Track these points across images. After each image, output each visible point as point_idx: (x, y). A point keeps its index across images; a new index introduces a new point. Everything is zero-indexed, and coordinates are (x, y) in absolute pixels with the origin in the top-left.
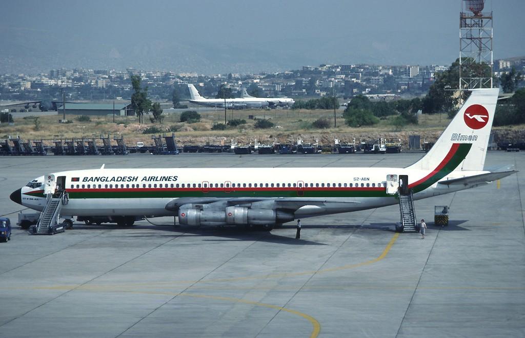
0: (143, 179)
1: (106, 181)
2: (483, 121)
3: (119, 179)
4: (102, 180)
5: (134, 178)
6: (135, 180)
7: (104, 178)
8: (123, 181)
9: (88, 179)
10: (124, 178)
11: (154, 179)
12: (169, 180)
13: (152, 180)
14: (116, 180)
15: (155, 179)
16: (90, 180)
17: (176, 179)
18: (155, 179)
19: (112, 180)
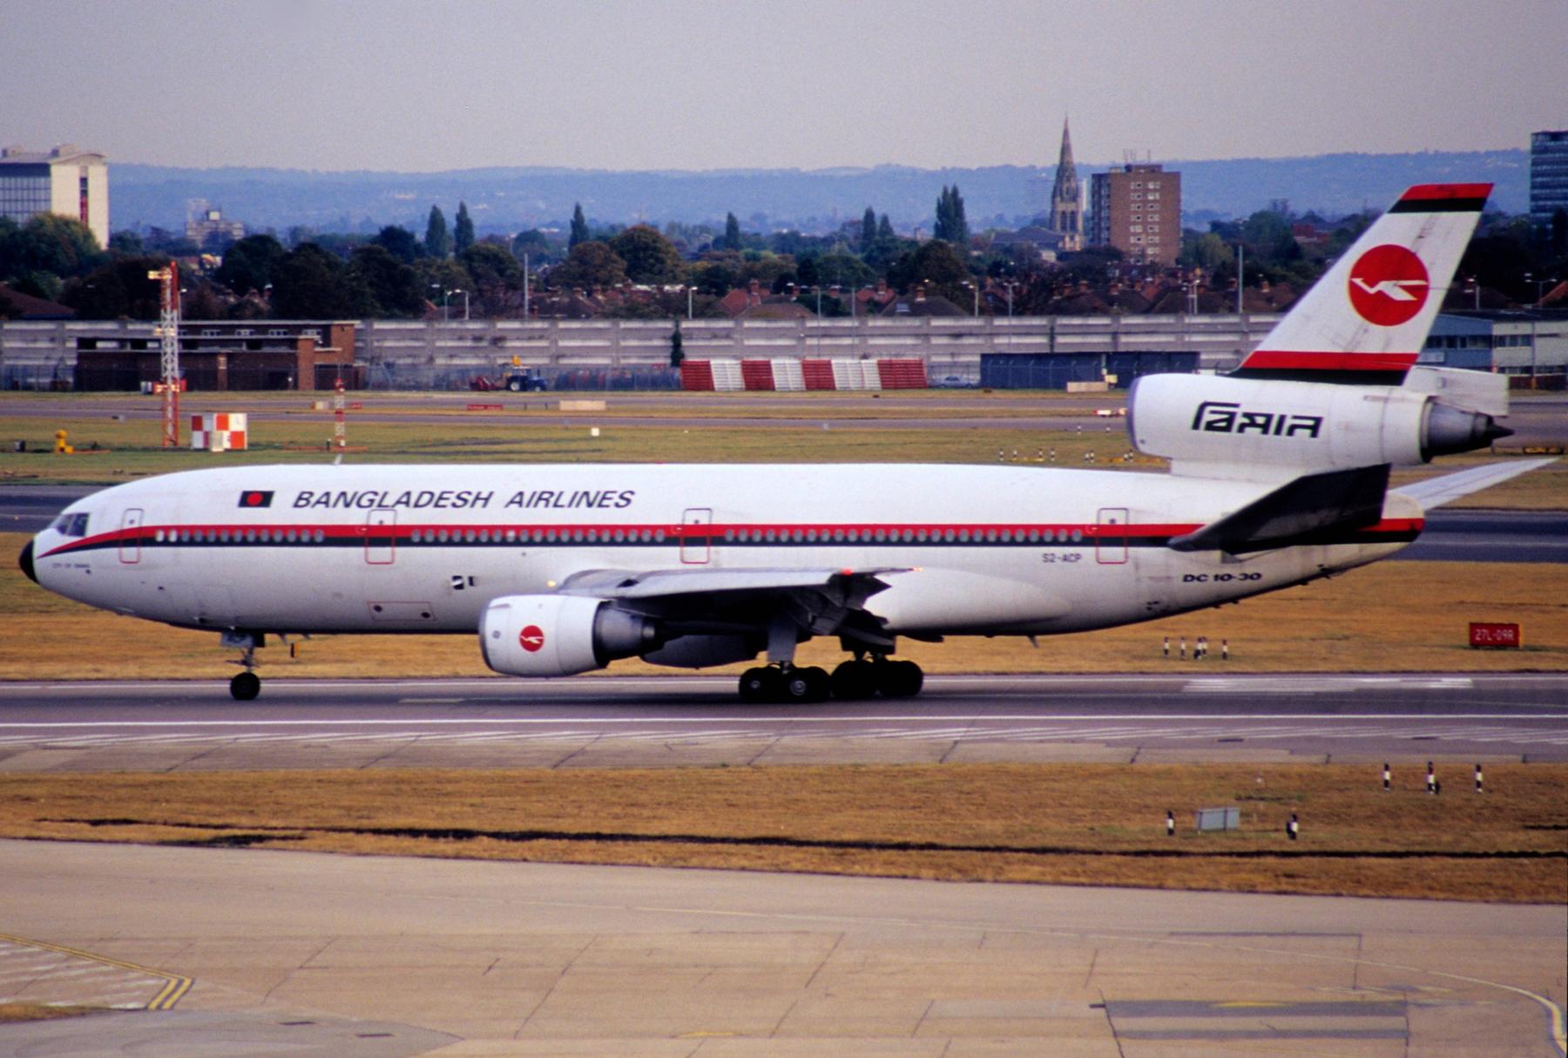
0: (512, 502)
3: (426, 498)
4: (364, 502)
5: (477, 498)
6: (480, 503)
7: (371, 496)
8: (436, 505)
9: (313, 500)
10: (441, 498)
12: (600, 505)
13: (542, 503)
14: (413, 500)
15: (552, 500)
16: (318, 502)
17: (628, 501)
18: (552, 500)
19: (399, 502)
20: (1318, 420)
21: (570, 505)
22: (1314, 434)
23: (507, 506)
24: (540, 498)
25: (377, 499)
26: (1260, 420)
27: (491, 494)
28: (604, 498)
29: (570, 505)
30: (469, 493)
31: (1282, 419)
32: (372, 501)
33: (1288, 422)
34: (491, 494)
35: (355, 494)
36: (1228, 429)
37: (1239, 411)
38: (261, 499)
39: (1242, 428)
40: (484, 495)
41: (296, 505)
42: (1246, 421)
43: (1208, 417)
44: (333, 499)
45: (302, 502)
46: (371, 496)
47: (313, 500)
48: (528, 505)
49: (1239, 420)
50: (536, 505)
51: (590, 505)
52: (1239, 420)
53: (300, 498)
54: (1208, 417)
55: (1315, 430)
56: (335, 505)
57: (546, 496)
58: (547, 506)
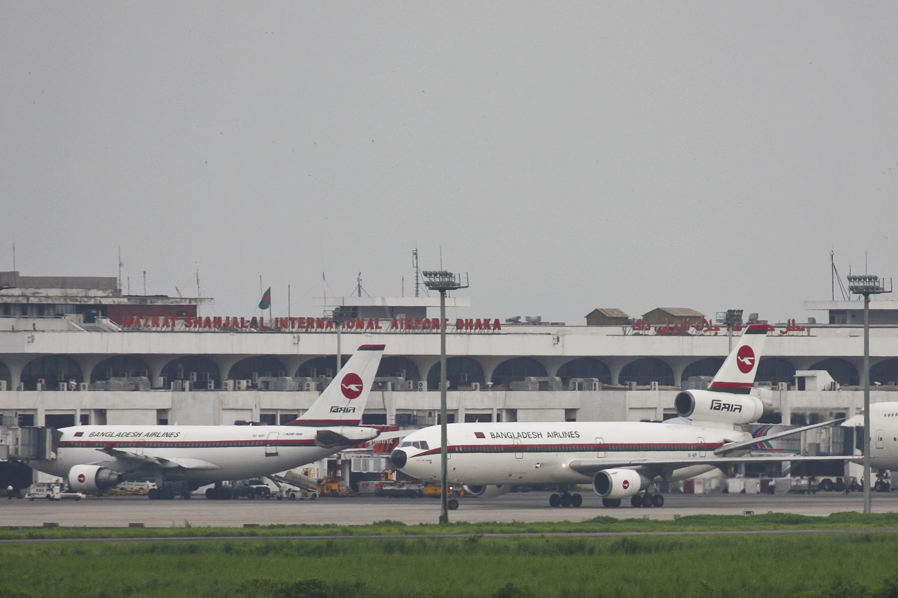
20: (741, 406)
22: (740, 412)
26: (727, 406)
31: (732, 405)
33: (734, 407)
36: (719, 409)
37: (722, 403)
38: (480, 435)
39: (723, 408)
42: (724, 406)
43: (715, 405)
49: (722, 406)
52: (722, 406)
54: (715, 405)
55: (740, 409)
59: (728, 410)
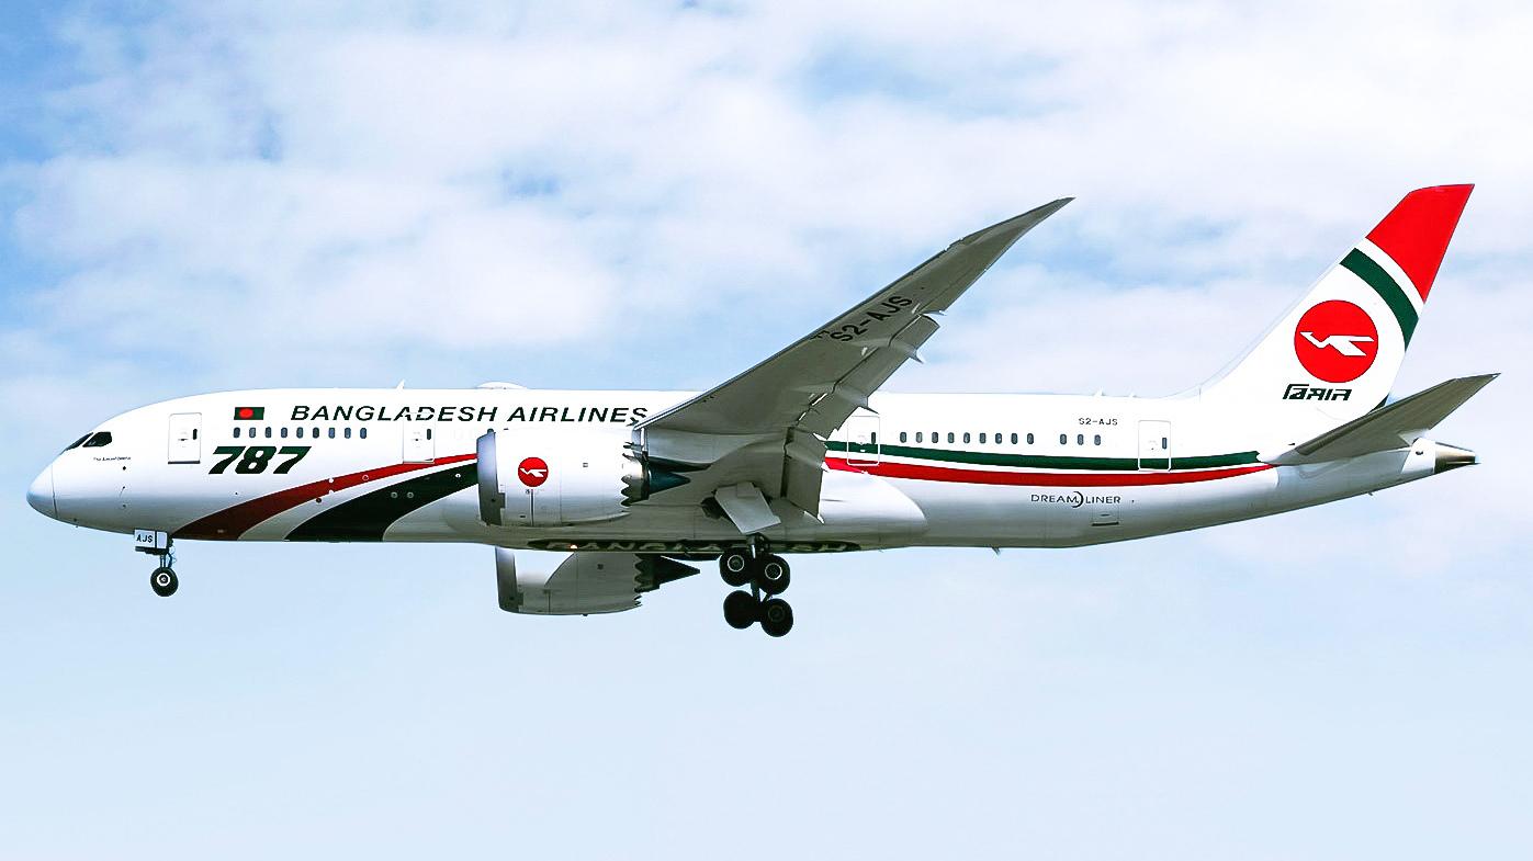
0: (513, 416)
1: (380, 418)
2: (1359, 353)
4: (362, 415)
5: (482, 412)
6: (486, 418)
7: (369, 410)
8: (440, 419)
9: (311, 413)
10: (442, 413)
11: (552, 415)
12: (613, 420)
13: (548, 419)
15: (559, 416)
16: (317, 415)
18: (559, 416)
19: (400, 415)
21: (581, 419)
23: (510, 420)
24: (543, 414)
25: (376, 413)
26: (1319, 392)
27: (495, 409)
28: (615, 414)
29: (581, 419)
30: (472, 409)
32: (371, 415)
34: (495, 409)
35: (351, 408)
40: (489, 409)
41: (293, 418)
44: (331, 414)
45: (298, 416)
46: (369, 410)
47: (311, 413)
48: (532, 419)
50: (541, 419)
51: (602, 419)
52: (1309, 392)
53: (295, 412)
56: (335, 418)
57: (548, 412)
58: (554, 419)
59: (1320, 399)
